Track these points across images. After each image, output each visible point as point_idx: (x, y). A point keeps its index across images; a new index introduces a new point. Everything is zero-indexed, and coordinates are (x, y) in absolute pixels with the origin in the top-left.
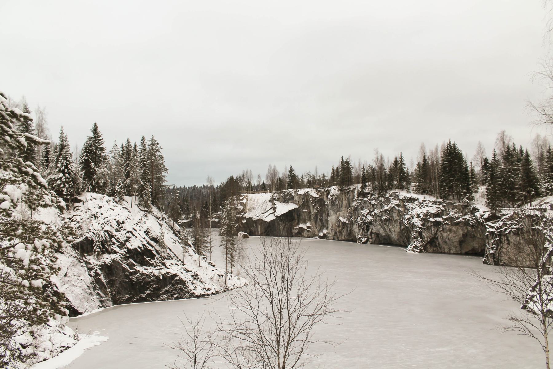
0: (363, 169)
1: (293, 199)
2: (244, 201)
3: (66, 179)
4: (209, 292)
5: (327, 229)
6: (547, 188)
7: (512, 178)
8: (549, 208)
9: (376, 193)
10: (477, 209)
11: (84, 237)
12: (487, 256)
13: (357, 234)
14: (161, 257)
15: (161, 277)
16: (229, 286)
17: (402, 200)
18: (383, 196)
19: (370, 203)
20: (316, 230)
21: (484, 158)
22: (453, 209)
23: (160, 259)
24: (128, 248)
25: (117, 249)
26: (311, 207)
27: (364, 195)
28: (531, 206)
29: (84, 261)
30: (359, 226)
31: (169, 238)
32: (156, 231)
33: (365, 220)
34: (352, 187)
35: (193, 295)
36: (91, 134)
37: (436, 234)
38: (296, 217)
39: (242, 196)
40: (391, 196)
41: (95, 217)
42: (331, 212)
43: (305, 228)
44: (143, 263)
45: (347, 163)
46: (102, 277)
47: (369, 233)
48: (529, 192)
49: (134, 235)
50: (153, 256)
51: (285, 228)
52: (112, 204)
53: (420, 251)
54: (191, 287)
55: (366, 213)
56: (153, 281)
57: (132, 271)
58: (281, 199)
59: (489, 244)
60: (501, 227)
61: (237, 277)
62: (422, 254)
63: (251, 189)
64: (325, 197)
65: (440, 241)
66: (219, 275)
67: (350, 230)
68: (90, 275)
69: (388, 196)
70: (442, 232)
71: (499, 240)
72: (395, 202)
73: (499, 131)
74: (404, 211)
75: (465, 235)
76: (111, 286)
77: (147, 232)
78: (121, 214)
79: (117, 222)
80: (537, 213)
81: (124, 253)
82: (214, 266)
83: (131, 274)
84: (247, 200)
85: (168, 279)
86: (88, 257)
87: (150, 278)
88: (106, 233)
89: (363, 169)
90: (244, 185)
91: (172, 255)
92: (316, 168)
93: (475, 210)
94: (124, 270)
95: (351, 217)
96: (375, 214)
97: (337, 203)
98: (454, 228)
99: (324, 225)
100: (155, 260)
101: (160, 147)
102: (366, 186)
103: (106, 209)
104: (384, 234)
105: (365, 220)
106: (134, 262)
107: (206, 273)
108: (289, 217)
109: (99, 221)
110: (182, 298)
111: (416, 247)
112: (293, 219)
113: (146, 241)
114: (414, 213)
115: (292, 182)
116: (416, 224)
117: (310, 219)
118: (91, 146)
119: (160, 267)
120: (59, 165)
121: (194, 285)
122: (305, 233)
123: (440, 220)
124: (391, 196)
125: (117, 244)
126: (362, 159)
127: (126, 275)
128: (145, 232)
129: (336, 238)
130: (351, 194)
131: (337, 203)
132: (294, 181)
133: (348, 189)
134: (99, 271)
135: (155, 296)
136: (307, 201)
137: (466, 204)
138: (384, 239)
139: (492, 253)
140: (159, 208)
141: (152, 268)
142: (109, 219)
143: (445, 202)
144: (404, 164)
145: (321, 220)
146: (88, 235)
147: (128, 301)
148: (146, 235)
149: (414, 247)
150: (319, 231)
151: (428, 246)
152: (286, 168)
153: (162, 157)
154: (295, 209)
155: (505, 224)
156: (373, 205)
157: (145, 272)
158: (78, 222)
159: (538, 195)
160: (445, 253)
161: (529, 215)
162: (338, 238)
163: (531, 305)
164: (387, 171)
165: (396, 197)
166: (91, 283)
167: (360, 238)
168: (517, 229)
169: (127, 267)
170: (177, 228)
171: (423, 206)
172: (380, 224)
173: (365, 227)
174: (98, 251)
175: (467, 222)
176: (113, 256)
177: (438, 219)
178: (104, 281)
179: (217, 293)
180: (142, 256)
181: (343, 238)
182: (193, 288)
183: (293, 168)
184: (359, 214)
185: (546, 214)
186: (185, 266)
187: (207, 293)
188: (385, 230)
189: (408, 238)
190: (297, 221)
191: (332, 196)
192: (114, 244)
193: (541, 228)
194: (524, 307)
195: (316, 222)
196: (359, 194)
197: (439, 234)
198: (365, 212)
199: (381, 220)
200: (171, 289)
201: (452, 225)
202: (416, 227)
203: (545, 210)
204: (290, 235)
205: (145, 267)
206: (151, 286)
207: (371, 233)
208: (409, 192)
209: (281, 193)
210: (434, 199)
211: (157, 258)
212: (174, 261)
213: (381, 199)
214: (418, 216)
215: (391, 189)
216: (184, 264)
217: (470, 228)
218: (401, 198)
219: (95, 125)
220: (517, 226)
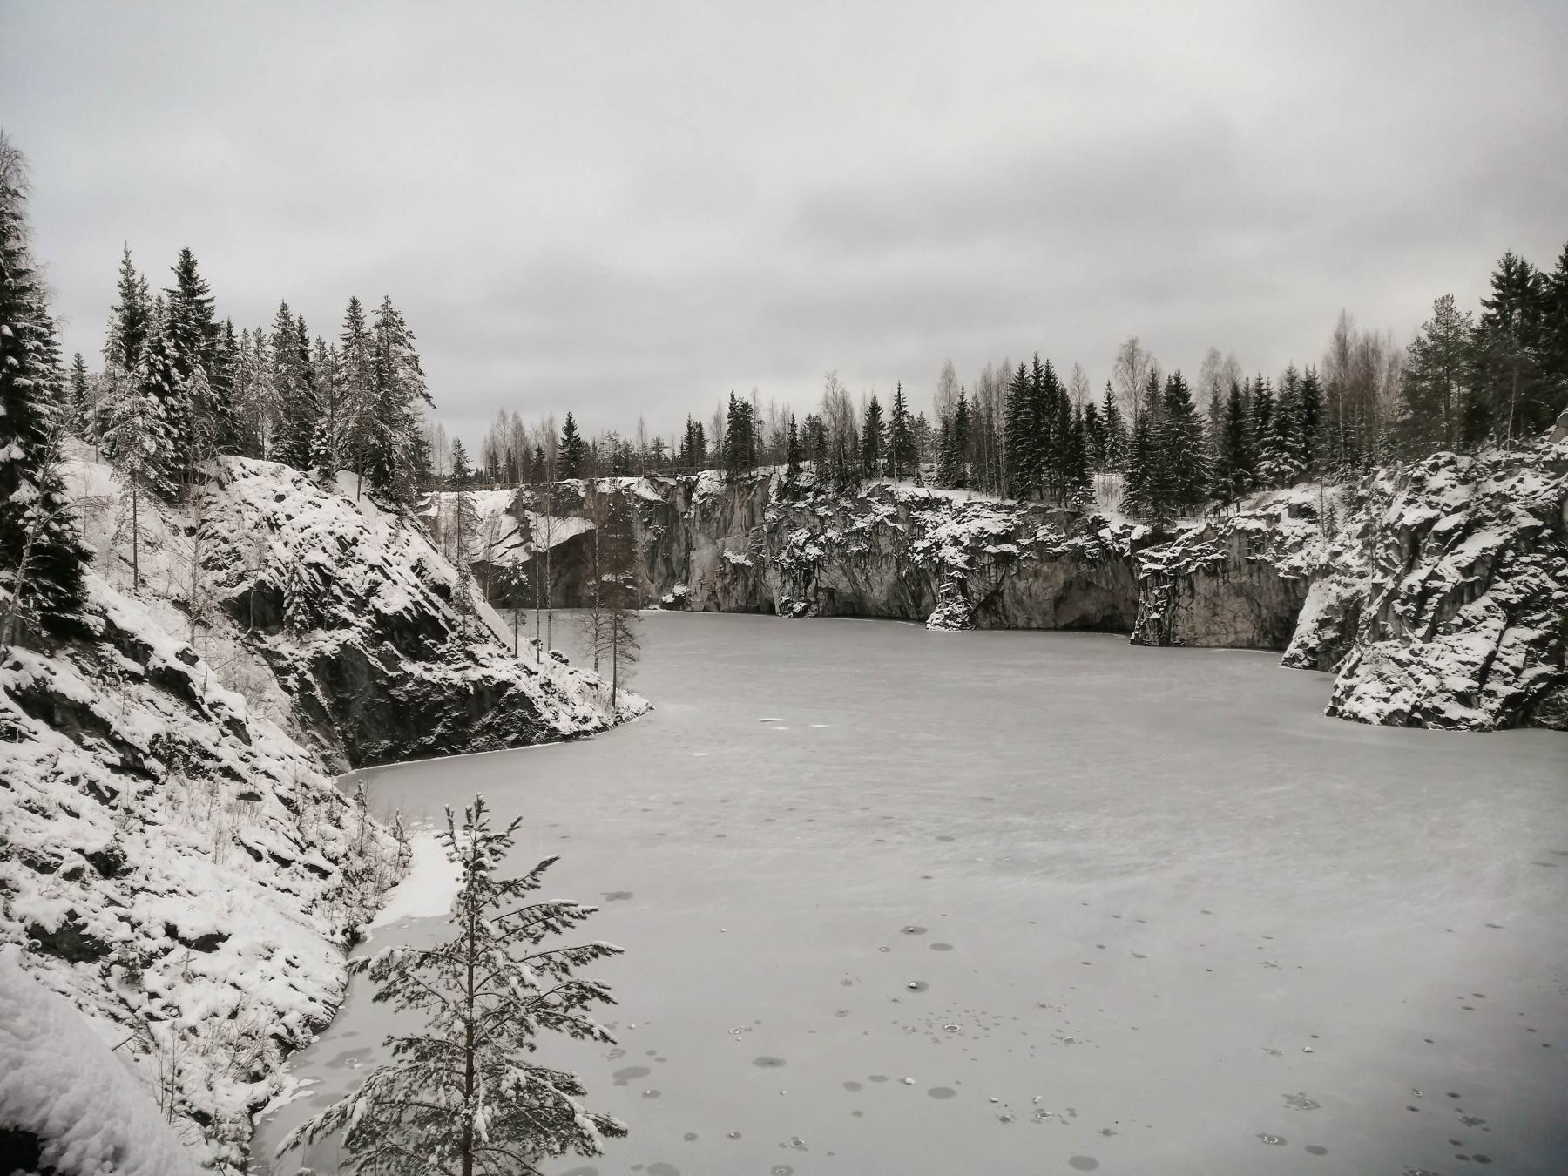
1: (581, 506)
2: (432, 512)
3: (167, 410)
4: (589, 727)
5: (686, 582)
6: (1269, 471)
7: (1188, 447)
8: (1285, 513)
9: (831, 487)
11: (251, 583)
12: (1143, 628)
13: (775, 594)
14: (460, 637)
15: (471, 690)
18: (852, 496)
19: (814, 513)
20: (653, 588)
21: (1086, 403)
23: (458, 642)
24: (377, 611)
25: (351, 617)
27: (799, 494)
29: (258, 649)
30: (785, 571)
33: (800, 558)
34: (761, 472)
35: (553, 735)
36: (174, 283)
39: (424, 498)
40: (870, 495)
41: (271, 525)
44: (418, 654)
46: (318, 692)
48: (1238, 478)
49: (388, 578)
50: (440, 635)
51: (560, 585)
52: (310, 492)
53: (963, 625)
55: (802, 539)
56: (449, 700)
59: (1147, 598)
60: (1176, 560)
64: (680, 501)
65: (1007, 599)
67: (755, 585)
71: (1173, 588)
72: (884, 510)
73: (1125, 341)
74: (910, 532)
75: (1068, 585)
77: (419, 569)
78: (342, 518)
79: (340, 539)
80: (1262, 525)
82: (566, 662)
83: (393, 682)
85: (487, 695)
87: (441, 692)
88: (313, 571)
89: (793, 425)
92: (642, 423)
93: (1099, 523)
95: (759, 550)
97: (718, 514)
98: (1045, 568)
100: (448, 645)
101: (409, 334)
104: (849, 591)
105: (800, 558)
108: (570, 551)
109: (287, 538)
110: (529, 743)
111: (952, 616)
114: (943, 533)
115: (575, 459)
116: (952, 562)
120: (144, 368)
123: (1012, 548)
124: (870, 495)
125: (348, 600)
126: (788, 399)
128: (413, 569)
129: (714, 605)
130: (759, 491)
131: (718, 514)
132: (576, 456)
133: (751, 478)
134: (309, 676)
136: (626, 509)
138: (846, 603)
143: (1023, 507)
145: (667, 561)
146: (262, 576)
147: (390, 756)
148: (418, 575)
149: (947, 617)
150: (660, 591)
151: (979, 612)
154: (588, 533)
155: (1186, 553)
156: (822, 519)
157: (427, 676)
158: (225, 541)
159: (1256, 484)
160: (1017, 628)
161: (1242, 531)
163: (1350, 705)
165: (887, 497)
168: (1215, 562)
171: (963, 520)
172: (841, 567)
173: (800, 574)
174: (301, 622)
175: (1078, 554)
176: (343, 635)
177: (1006, 548)
178: (324, 703)
179: (605, 728)
180: (414, 632)
181: (733, 605)
183: (577, 421)
184: (781, 541)
185: (1280, 527)
187: (583, 727)
188: (854, 581)
191: (702, 497)
192: (340, 601)
193: (1269, 558)
194: (1333, 712)
195: (652, 567)
196: (784, 491)
197: (1007, 583)
198: (800, 536)
199: (844, 555)
202: (953, 568)
203: (1278, 518)
207: (817, 589)
208: (920, 485)
209: (544, 489)
210: (996, 501)
211: (453, 641)
212: (490, 647)
213: (843, 502)
214: (956, 541)
215: (870, 477)
217: (1084, 568)
219: (187, 254)
220: (1215, 556)
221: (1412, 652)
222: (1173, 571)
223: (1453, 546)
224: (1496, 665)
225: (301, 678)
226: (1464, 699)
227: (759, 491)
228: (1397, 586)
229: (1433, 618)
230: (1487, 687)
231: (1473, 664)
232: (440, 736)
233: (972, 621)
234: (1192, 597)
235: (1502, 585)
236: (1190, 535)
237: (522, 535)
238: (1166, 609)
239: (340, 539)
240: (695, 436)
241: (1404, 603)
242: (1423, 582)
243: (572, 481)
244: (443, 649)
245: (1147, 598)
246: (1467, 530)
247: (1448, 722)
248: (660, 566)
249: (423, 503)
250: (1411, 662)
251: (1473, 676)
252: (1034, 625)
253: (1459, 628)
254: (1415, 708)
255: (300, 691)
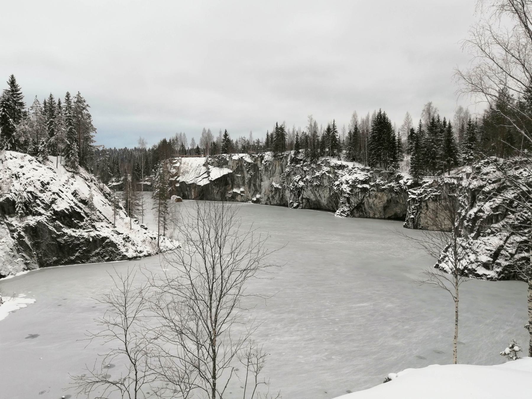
0: (297, 135)
2: (178, 165)
4: (141, 255)
5: (260, 193)
6: (465, 159)
7: (435, 148)
8: (465, 177)
9: (309, 160)
10: (401, 177)
11: (4, 198)
12: (408, 221)
13: (288, 199)
14: (90, 220)
15: (91, 240)
16: (161, 248)
17: (332, 167)
18: (315, 163)
19: (302, 169)
20: (250, 195)
21: (411, 128)
22: (379, 177)
23: (89, 221)
24: (54, 210)
25: (42, 211)
26: (245, 172)
28: (449, 175)
29: (5, 223)
30: (291, 191)
31: (98, 200)
32: (85, 193)
33: (296, 186)
36: (8, 87)
37: (363, 200)
38: (230, 182)
39: (175, 160)
40: (322, 163)
42: (265, 178)
43: (239, 192)
45: (282, 129)
46: (26, 239)
47: (300, 198)
48: (448, 162)
49: (60, 197)
50: (82, 219)
52: (35, 164)
53: (348, 215)
54: (123, 250)
56: (82, 243)
57: (59, 233)
58: (216, 164)
59: (410, 209)
60: (421, 194)
61: (170, 240)
62: (349, 218)
63: (185, 153)
64: (259, 163)
65: (366, 206)
66: (151, 238)
67: (282, 195)
68: (13, 238)
69: (319, 162)
70: (368, 198)
72: (326, 169)
75: (389, 201)
76: (37, 249)
77: (75, 194)
78: (45, 174)
79: (42, 182)
81: (51, 215)
82: (146, 229)
83: (59, 236)
84: (181, 163)
85: (98, 242)
86: (10, 219)
88: (29, 194)
89: (297, 135)
90: (178, 148)
91: (103, 218)
93: (400, 177)
94: (51, 232)
95: (284, 182)
96: (307, 180)
97: (271, 168)
98: (379, 195)
99: (257, 191)
100: (84, 223)
101: (87, 105)
102: (299, 153)
103: (28, 169)
104: (314, 199)
105: (296, 186)
106: (61, 225)
107: (138, 236)
108: (223, 181)
109: (21, 182)
110: (113, 260)
111: (343, 212)
112: (227, 184)
113: (74, 203)
114: (343, 179)
115: (227, 147)
117: (244, 184)
118: (8, 100)
119: (89, 230)
121: (126, 248)
122: (239, 198)
123: (367, 186)
124: (322, 163)
125: (43, 205)
127: (53, 238)
128: (72, 194)
129: (269, 202)
130: (285, 160)
132: (228, 146)
133: (282, 155)
134: (22, 233)
135: (84, 258)
136: (241, 166)
137: (392, 172)
138: (314, 204)
139: (412, 218)
140: (87, 169)
141: (81, 230)
142: (32, 179)
143: (372, 170)
144: (336, 131)
145: (255, 185)
146: (8, 196)
147: (56, 263)
148: (74, 196)
149: (342, 212)
150: (252, 196)
151: (355, 211)
152: (220, 132)
153: (89, 116)
154: (229, 174)
156: (305, 172)
157: (73, 234)
159: (457, 164)
160: (370, 218)
162: (270, 202)
163: (443, 265)
164: (320, 138)
165: (328, 164)
166: (14, 246)
167: (292, 202)
168: (436, 196)
169: (54, 229)
170: (107, 189)
171: (352, 173)
172: (311, 190)
173: (296, 192)
174: (21, 213)
175: (391, 189)
176: (38, 218)
178: (29, 243)
179: (149, 255)
180: (70, 218)
181: (275, 203)
182: (125, 250)
183: (228, 133)
186: (116, 229)
187: (139, 255)
188: (315, 196)
189: (337, 203)
190: (231, 186)
191: (266, 162)
192: (39, 205)
194: (437, 266)
195: (249, 187)
197: (365, 199)
198: (297, 178)
199: (312, 186)
200: (102, 251)
201: (378, 191)
202: (345, 193)
203: (461, 179)
204: (224, 199)
205: (73, 229)
206: (81, 248)
207: (302, 198)
208: (339, 159)
209: (215, 157)
212: (104, 224)
213: (313, 166)
214: (347, 182)
215: (323, 156)
216: (115, 227)
217: (394, 195)
218: (332, 165)
219: (12, 77)
220: (436, 193)
221: (468, 243)
222: (420, 199)
223: (491, 198)
224: (503, 252)
225: (19, 234)
226: (486, 266)
227: (285, 160)
228: (466, 214)
229: (478, 229)
230: (498, 261)
231: (491, 251)
232: (77, 256)
233: (352, 214)
234: (427, 209)
235: (512, 216)
236: (427, 184)
237: (208, 174)
238: (416, 214)
239: (42, 182)
240: (270, 139)
241: (468, 222)
242: (476, 213)
243: (225, 155)
244: (82, 224)
245: (410, 209)
246: (499, 191)
247: (478, 275)
248: (252, 187)
249: (175, 161)
250: (468, 248)
251: (491, 256)
252: (376, 216)
253: (489, 234)
254: (466, 268)
255: (18, 239)
